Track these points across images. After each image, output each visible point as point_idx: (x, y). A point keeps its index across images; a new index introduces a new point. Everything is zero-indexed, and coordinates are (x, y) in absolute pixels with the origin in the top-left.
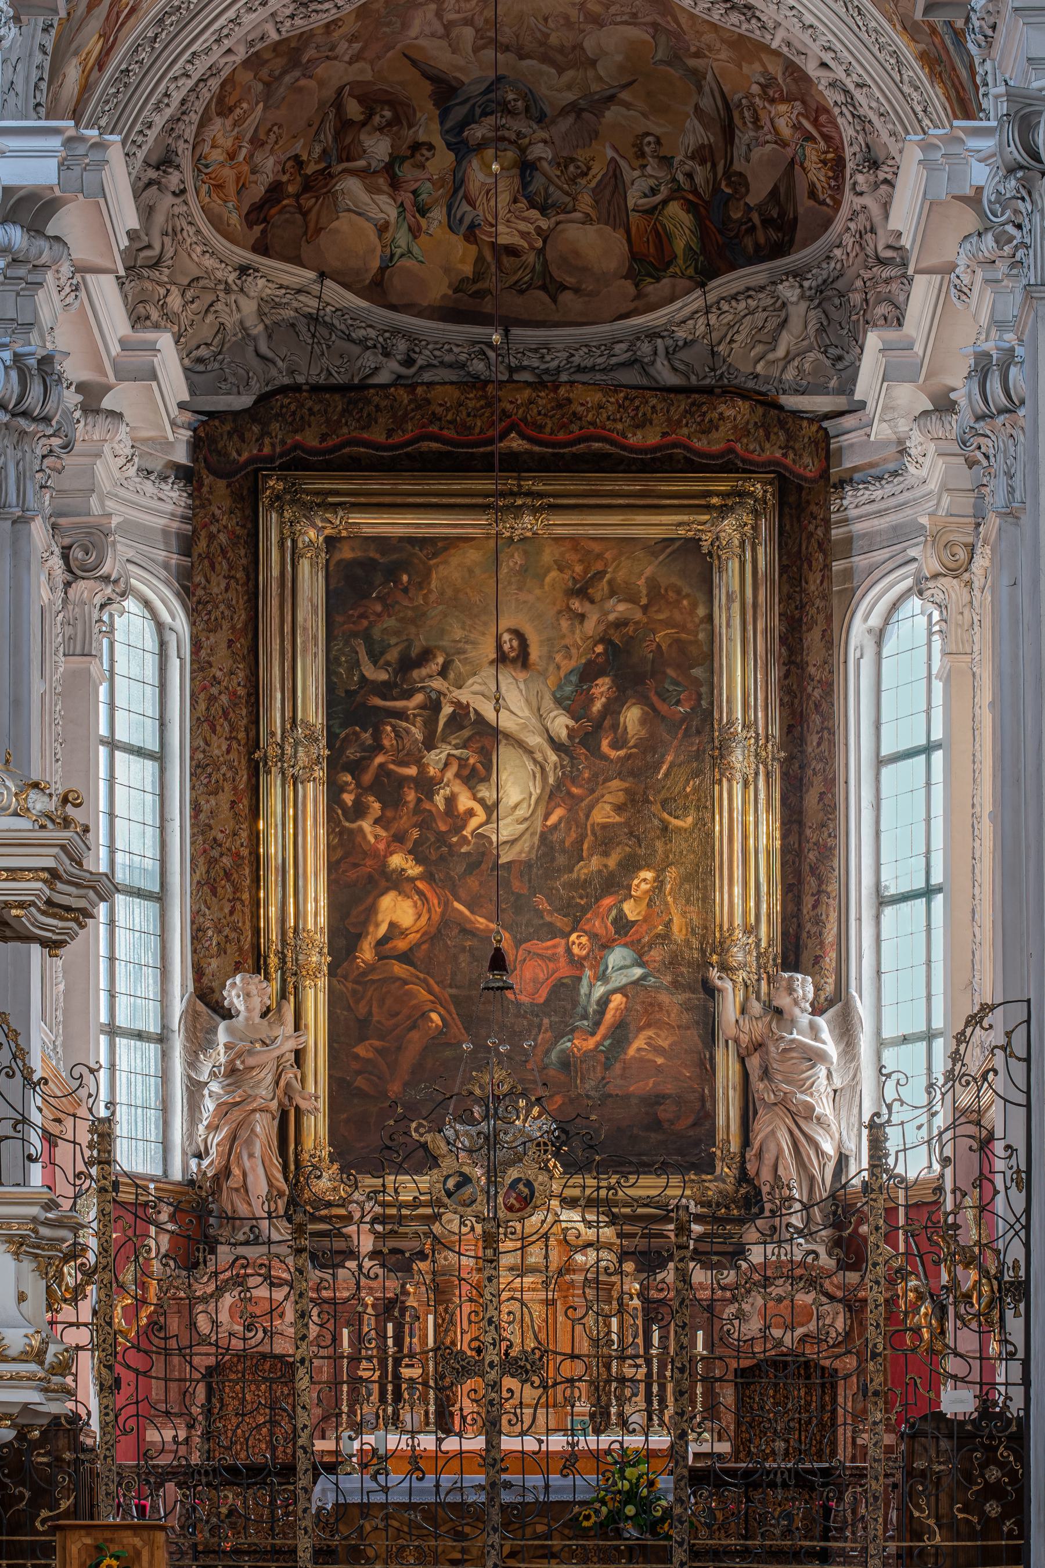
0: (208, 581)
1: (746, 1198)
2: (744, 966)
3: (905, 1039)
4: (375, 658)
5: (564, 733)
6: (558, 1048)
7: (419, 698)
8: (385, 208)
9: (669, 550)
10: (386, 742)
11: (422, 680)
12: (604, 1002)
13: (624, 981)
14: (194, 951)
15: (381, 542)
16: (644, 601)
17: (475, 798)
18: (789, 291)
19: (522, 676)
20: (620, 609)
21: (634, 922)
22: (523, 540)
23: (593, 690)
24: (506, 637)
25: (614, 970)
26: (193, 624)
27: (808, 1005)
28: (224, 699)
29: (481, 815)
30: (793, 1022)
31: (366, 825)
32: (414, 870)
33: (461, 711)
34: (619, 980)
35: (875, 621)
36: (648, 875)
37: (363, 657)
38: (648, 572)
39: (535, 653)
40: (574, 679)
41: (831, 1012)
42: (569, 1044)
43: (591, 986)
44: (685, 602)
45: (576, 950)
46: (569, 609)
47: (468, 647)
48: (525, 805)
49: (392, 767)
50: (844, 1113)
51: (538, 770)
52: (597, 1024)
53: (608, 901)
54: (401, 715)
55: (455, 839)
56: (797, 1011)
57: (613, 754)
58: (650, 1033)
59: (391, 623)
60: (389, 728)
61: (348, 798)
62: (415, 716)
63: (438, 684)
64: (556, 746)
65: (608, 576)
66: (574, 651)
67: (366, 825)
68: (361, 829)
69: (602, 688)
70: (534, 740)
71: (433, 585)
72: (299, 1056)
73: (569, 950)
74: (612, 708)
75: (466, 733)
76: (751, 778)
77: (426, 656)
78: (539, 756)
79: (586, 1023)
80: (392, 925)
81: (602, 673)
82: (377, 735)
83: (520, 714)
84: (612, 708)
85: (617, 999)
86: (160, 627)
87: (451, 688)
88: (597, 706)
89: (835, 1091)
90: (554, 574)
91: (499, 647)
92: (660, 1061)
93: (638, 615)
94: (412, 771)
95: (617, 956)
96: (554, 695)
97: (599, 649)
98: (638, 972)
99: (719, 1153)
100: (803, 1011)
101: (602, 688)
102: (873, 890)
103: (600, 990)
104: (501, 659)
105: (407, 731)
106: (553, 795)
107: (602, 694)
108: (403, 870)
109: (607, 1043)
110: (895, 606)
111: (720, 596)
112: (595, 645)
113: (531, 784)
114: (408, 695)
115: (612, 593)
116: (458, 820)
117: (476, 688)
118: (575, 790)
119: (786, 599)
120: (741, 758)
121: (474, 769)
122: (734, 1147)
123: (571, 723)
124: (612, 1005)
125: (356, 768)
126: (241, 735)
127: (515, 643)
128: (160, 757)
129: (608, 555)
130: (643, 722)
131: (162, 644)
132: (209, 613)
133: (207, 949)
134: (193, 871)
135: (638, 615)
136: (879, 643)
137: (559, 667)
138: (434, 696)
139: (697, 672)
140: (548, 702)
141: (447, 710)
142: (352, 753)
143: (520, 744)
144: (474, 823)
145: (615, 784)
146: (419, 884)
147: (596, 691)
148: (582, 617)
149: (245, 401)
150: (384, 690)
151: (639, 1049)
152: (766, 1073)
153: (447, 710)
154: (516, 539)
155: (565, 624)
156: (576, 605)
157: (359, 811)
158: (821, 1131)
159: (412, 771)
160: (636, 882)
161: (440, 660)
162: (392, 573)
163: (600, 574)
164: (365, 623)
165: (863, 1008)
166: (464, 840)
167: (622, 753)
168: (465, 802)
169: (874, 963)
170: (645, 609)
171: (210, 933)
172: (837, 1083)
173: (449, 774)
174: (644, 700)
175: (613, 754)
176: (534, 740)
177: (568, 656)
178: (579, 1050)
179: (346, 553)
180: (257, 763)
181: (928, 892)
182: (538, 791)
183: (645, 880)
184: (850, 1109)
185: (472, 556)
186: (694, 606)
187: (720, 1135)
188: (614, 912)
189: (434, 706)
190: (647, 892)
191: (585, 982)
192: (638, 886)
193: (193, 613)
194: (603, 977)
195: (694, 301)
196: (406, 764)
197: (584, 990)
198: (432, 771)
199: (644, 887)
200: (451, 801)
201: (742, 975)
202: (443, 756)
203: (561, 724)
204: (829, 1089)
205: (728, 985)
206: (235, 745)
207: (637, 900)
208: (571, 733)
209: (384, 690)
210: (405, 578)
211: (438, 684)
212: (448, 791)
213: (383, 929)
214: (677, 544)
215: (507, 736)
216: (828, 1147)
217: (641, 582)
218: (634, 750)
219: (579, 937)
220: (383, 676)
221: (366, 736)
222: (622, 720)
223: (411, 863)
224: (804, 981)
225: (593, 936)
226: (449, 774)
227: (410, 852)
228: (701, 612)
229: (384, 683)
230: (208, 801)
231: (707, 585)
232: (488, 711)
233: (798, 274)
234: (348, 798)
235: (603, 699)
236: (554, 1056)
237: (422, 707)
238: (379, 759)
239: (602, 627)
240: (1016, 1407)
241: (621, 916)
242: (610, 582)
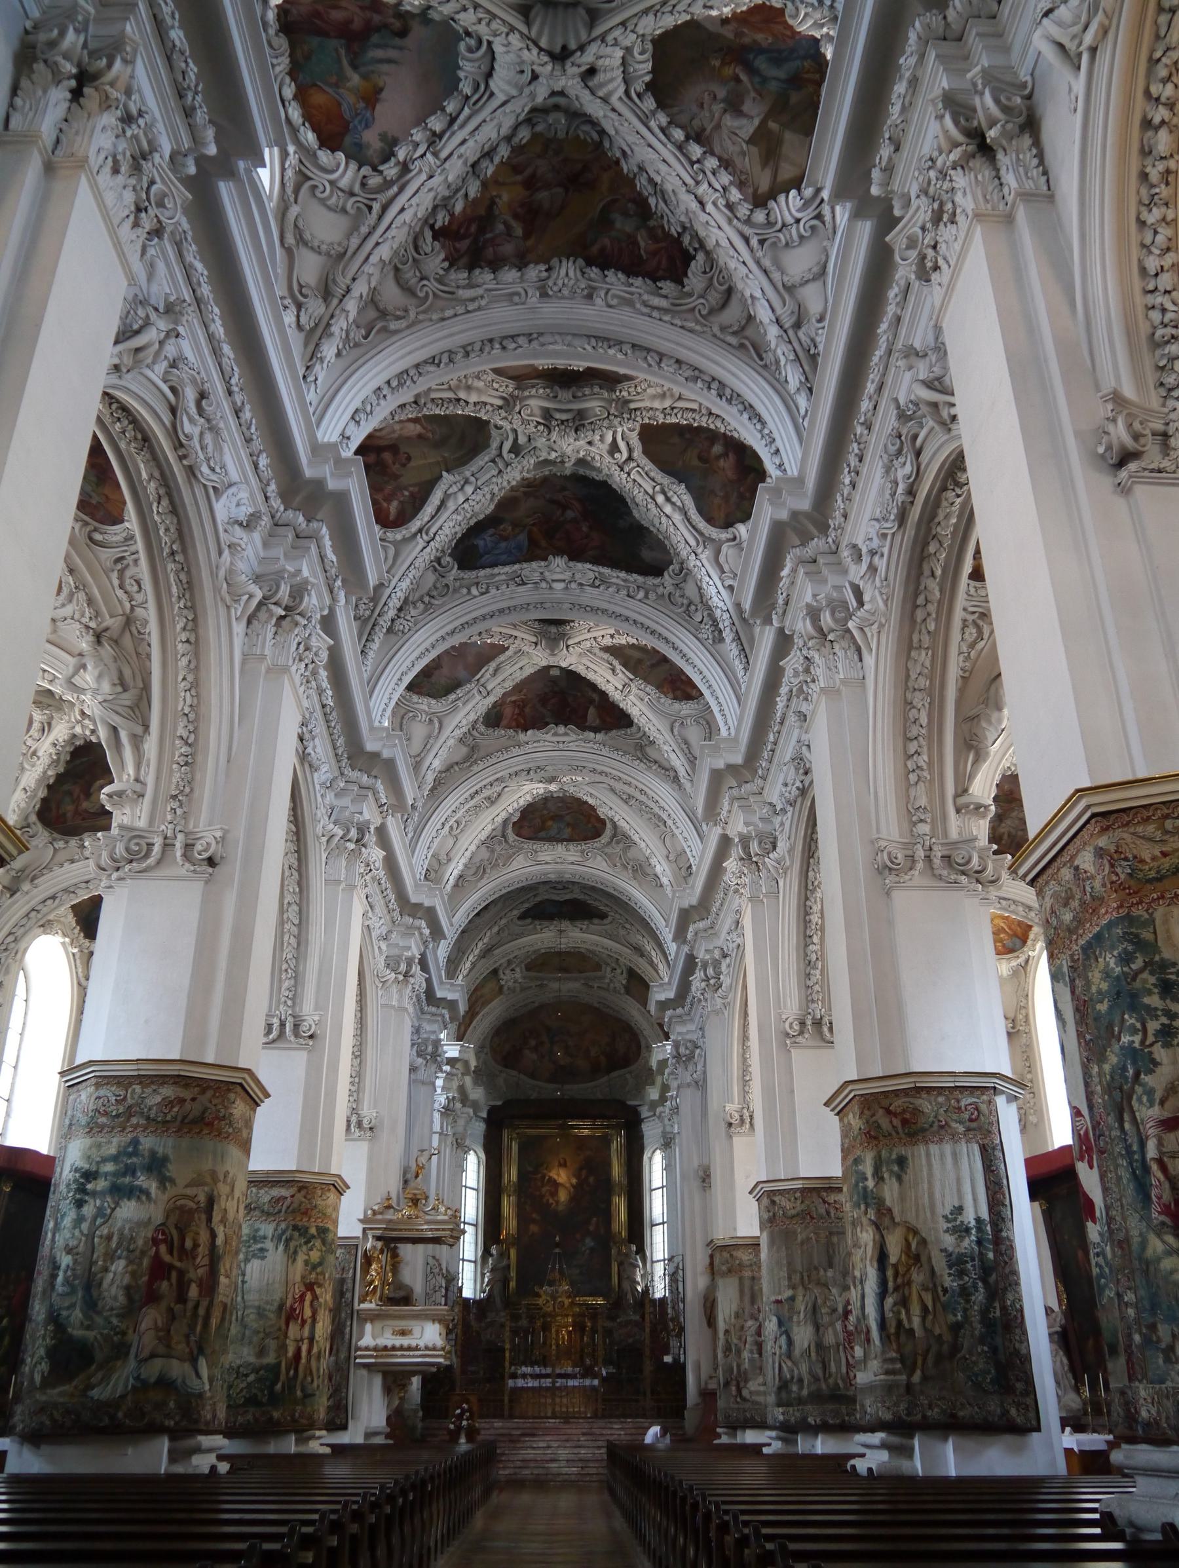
8: (534, 1056)
18: (628, 1076)
33: (550, 1178)
72: (509, 1266)
86: (478, 1157)
101: (584, 1173)
104: (560, 1165)
106: (573, 1199)
116: (548, 1205)
128: (477, 1190)
149: (499, 1103)
165: (648, 1254)
168: (551, 1201)
181: (663, 1223)
189: (544, 1177)
195: (605, 1079)
203: (574, 1181)
232: (556, 1177)
233: (630, 1072)
240: (682, 1360)
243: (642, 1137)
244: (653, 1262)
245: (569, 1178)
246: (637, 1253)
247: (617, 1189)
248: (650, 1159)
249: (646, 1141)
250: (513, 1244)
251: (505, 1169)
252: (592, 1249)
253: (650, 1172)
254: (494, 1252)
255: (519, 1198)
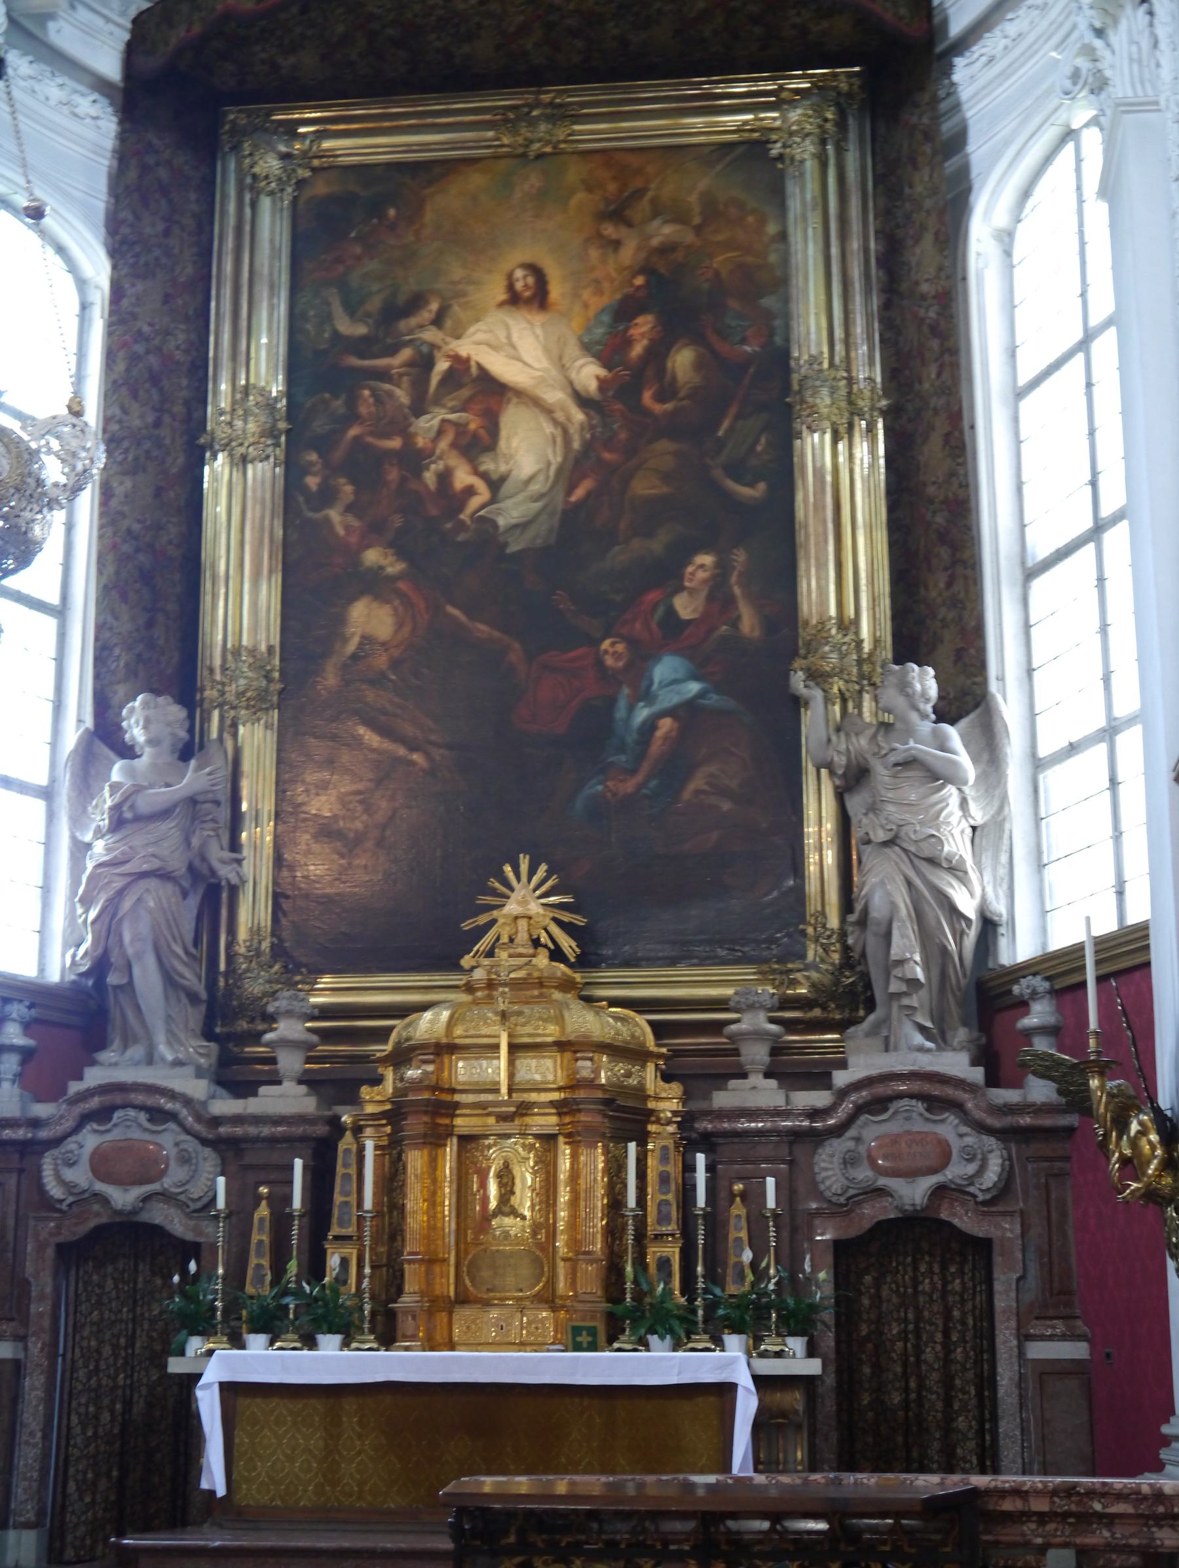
0: (138, 217)
1: (851, 990)
2: (840, 672)
3: (1073, 749)
4: (352, 310)
5: (593, 386)
6: (587, 791)
7: (406, 354)
9: (728, 158)
10: (363, 410)
11: (411, 332)
12: (650, 726)
13: (675, 700)
14: (97, 676)
15: (361, 171)
16: (697, 220)
17: (476, 472)
19: (538, 318)
20: (664, 232)
21: (689, 622)
22: (540, 156)
23: (632, 331)
24: (519, 273)
25: (663, 685)
26: (114, 267)
27: (929, 708)
28: (153, 361)
29: (483, 492)
30: (910, 732)
31: (334, 515)
32: (394, 567)
33: (460, 364)
34: (669, 699)
35: (1001, 218)
36: (706, 559)
37: (338, 310)
38: (704, 184)
39: (556, 291)
40: (606, 318)
41: (964, 723)
42: (600, 788)
43: (631, 708)
44: (750, 219)
45: (609, 661)
46: (599, 235)
47: (471, 288)
48: (541, 478)
49: (370, 439)
50: (986, 859)
51: (558, 433)
52: (641, 757)
53: (652, 596)
54: (383, 375)
55: (449, 525)
56: (914, 717)
57: (658, 408)
58: (712, 768)
59: (373, 266)
60: (366, 393)
61: (312, 482)
62: (401, 375)
63: (431, 335)
64: (583, 401)
65: (650, 194)
66: (606, 285)
67: (334, 515)
68: (327, 521)
69: (643, 327)
70: (555, 396)
71: (429, 216)
73: (599, 663)
74: (658, 353)
75: (465, 393)
76: (842, 429)
77: (416, 302)
78: (560, 416)
79: (623, 758)
80: (367, 640)
81: (642, 310)
82: (352, 402)
83: (536, 365)
84: (658, 353)
85: (666, 724)
86: (82, 283)
87: (448, 339)
88: (637, 350)
89: (974, 828)
90: (581, 196)
91: (510, 287)
92: (726, 806)
93: (689, 237)
94: (395, 443)
95: (665, 668)
96: (580, 339)
97: (639, 281)
98: (694, 687)
99: (810, 930)
100: (924, 716)
101: (643, 327)
102: (1018, 560)
103: (642, 713)
104: (514, 300)
105: (390, 395)
107: (643, 335)
108: (382, 568)
109: (653, 784)
110: (1026, 194)
111: (794, 205)
112: (634, 276)
113: (550, 451)
114: (393, 351)
115: (656, 213)
116: (452, 499)
117: (480, 336)
118: (608, 456)
119: (885, 213)
120: (828, 401)
121: (475, 436)
122: (834, 922)
123: (602, 372)
124: (659, 733)
125: (323, 445)
126: (179, 409)
127: (531, 280)
129: (650, 169)
130: (698, 365)
131: (84, 307)
132: (137, 255)
133: (113, 672)
134: (100, 572)
135: (689, 237)
136: (1008, 253)
137: (586, 306)
138: (425, 349)
139: (769, 302)
140: (573, 349)
141: (442, 365)
142: (320, 425)
143: (536, 403)
144: (474, 503)
145: (664, 445)
146: (402, 586)
147: (634, 332)
148: (616, 244)
150: (363, 347)
151: (698, 792)
152: (873, 809)
153: (442, 365)
154: (532, 155)
155: (594, 254)
156: (609, 230)
157: (326, 496)
158: (955, 883)
159: (395, 443)
160: (690, 569)
161: (434, 306)
162: (376, 208)
163: (639, 193)
164: (341, 269)
166: (462, 525)
167: (668, 406)
168: (463, 477)
169: (1022, 659)
170: (698, 229)
171: (117, 651)
172: (978, 815)
173: (443, 445)
174: (698, 339)
175: (658, 408)
176: (555, 396)
177: (599, 292)
178: (614, 795)
179: (321, 188)
180: (203, 449)
182: (559, 459)
183: (702, 566)
184: (996, 858)
185: (476, 180)
186: (762, 222)
187: (813, 906)
188: (660, 611)
189: (425, 362)
190: (705, 581)
191: (622, 704)
192: (692, 574)
193: (115, 253)
194: (647, 696)
196: (388, 436)
197: (620, 713)
198: (421, 442)
199: (702, 575)
200: (445, 477)
201: (837, 685)
202: (436, 422)
203: (589, 374)
204: (964, 824)
205: (818, 694)
206: (167, 419)
207: (692, 592)
208: (603, 383)
209: (363, 347)
210: (392, 212)
211: (431, 335)
212: (440, 465)
213: (352, 647)
214: (740, 150)
215: (520, 394)
216: (967, 905)
217: (693, 198)
218: (685, 403)
219: (613, 644)
220: (361, 330)
221: (338, 405)
222: (669, 365)
223: (391, 559)
224: (924, 673)
225: (632, 642)
226: (443, 445)
227: (391, 545)
228: (772, 229)
229: (364, 339)
230: (121, 483)
231: (778, 195)
234: (312, 482)
235: (645, 342)
236: (579, 803)
237: (410, 364)
238: (354, 432)
239: (643, 255)
241: (671, 612)
242: (653, 201)
243: (959, 140)
244: (1038, 765)
245: (563, 368)
246: (947, 712)
247: (823, 400)
248: (1006, 238)
249: (977, 149)
250: (258, 704)
251: (221, 339)
252: (687, 712)
253: (1010, 306)
254: (136, 733)
255: (293, 470)
